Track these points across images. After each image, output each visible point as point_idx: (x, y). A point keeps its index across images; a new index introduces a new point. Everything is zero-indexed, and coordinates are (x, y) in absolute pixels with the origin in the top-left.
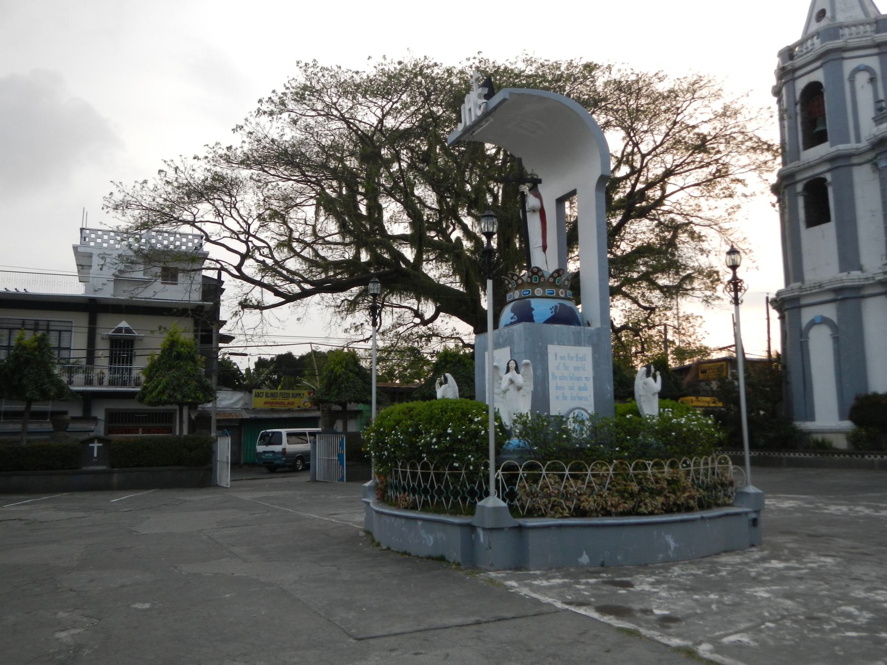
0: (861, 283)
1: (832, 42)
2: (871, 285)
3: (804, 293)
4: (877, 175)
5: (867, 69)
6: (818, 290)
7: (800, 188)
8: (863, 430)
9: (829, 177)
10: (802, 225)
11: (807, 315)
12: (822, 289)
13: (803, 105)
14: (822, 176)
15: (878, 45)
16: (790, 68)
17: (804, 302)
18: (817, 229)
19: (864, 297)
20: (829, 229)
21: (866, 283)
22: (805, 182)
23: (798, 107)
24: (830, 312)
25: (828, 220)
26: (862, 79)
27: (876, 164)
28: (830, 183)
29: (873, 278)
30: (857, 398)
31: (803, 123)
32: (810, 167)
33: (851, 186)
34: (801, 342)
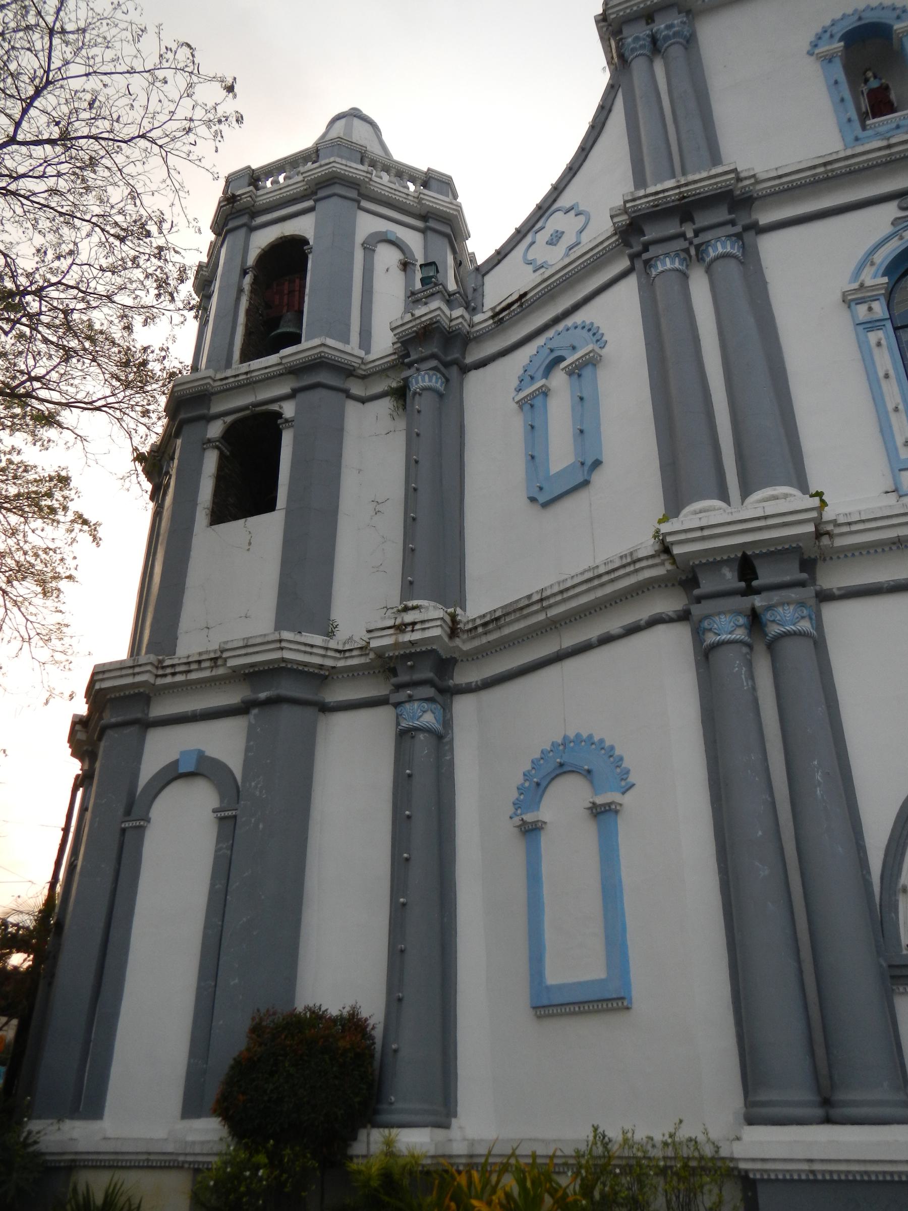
0: (329, 663)
1: (344, 162)
2: (352, 673)
3: (169, 680)
4: (401, 424)
6: (206, 674)
7: (215, 430)
8: (262, 1158)
9: (288, 410)
10: (202, 517)
12: (221, 671)
13: (255, 282)
14: (275, 407)
16: (246, 199)
17: (159, 710)
18: (235, 529)
19: (326, 709)
21: (341, 664)
22: (229, 419)
23: (248, 279)
25: (270, 506)
26: (387, 257)
27: (401, 394)
28: (287, 421)
29: (364, 649)
30: (256, 1030)
31: (248, 312)
32: (250, 383)
33: (339, 432)
34: (124, 831)
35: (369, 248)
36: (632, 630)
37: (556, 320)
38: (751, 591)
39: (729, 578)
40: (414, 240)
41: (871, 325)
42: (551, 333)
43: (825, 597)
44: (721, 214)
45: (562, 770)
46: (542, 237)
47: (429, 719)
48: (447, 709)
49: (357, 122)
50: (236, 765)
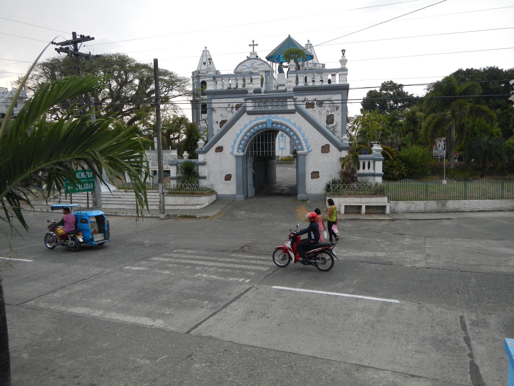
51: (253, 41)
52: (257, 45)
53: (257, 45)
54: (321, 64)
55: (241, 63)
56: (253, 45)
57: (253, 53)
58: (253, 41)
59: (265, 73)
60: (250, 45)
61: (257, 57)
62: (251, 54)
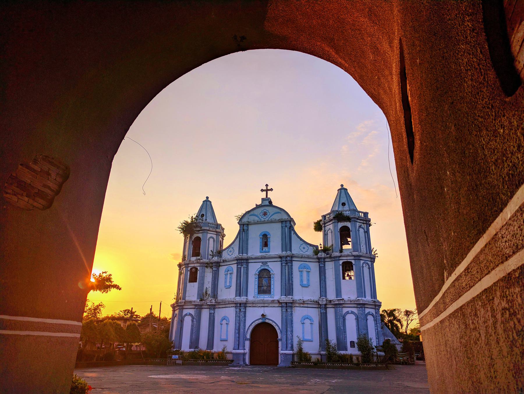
5: (213, 238)
11: (185, 312)
15: (217, 232)
19: (203, 308)
20: (196, 285)
24: (192, 312)
26: (211, 240)
35: (209, 240)
36: (231, 307)
37: (229, 265)
38: (240, 307)
39: (239, 305)
40: (215, 236)
41: (256, 278)
42: (229, 266)
43: (247, 307)
44: (245, 261)
45: (224, 319)
46: (230, 250)
47: (213, 312)
48: (215, 310)
49: (208, 202)
50: (193, 314)
51: (267, 185)
52: (271, 190)
53: (271, 190)
54: (362, 212)
55: (249, 212)
56: (267, 190)
57: (267, 199)
58: (267, 185)
59: (282, 224)
60: (262, 190)
61: (270, 202)
62: (263, 199)
